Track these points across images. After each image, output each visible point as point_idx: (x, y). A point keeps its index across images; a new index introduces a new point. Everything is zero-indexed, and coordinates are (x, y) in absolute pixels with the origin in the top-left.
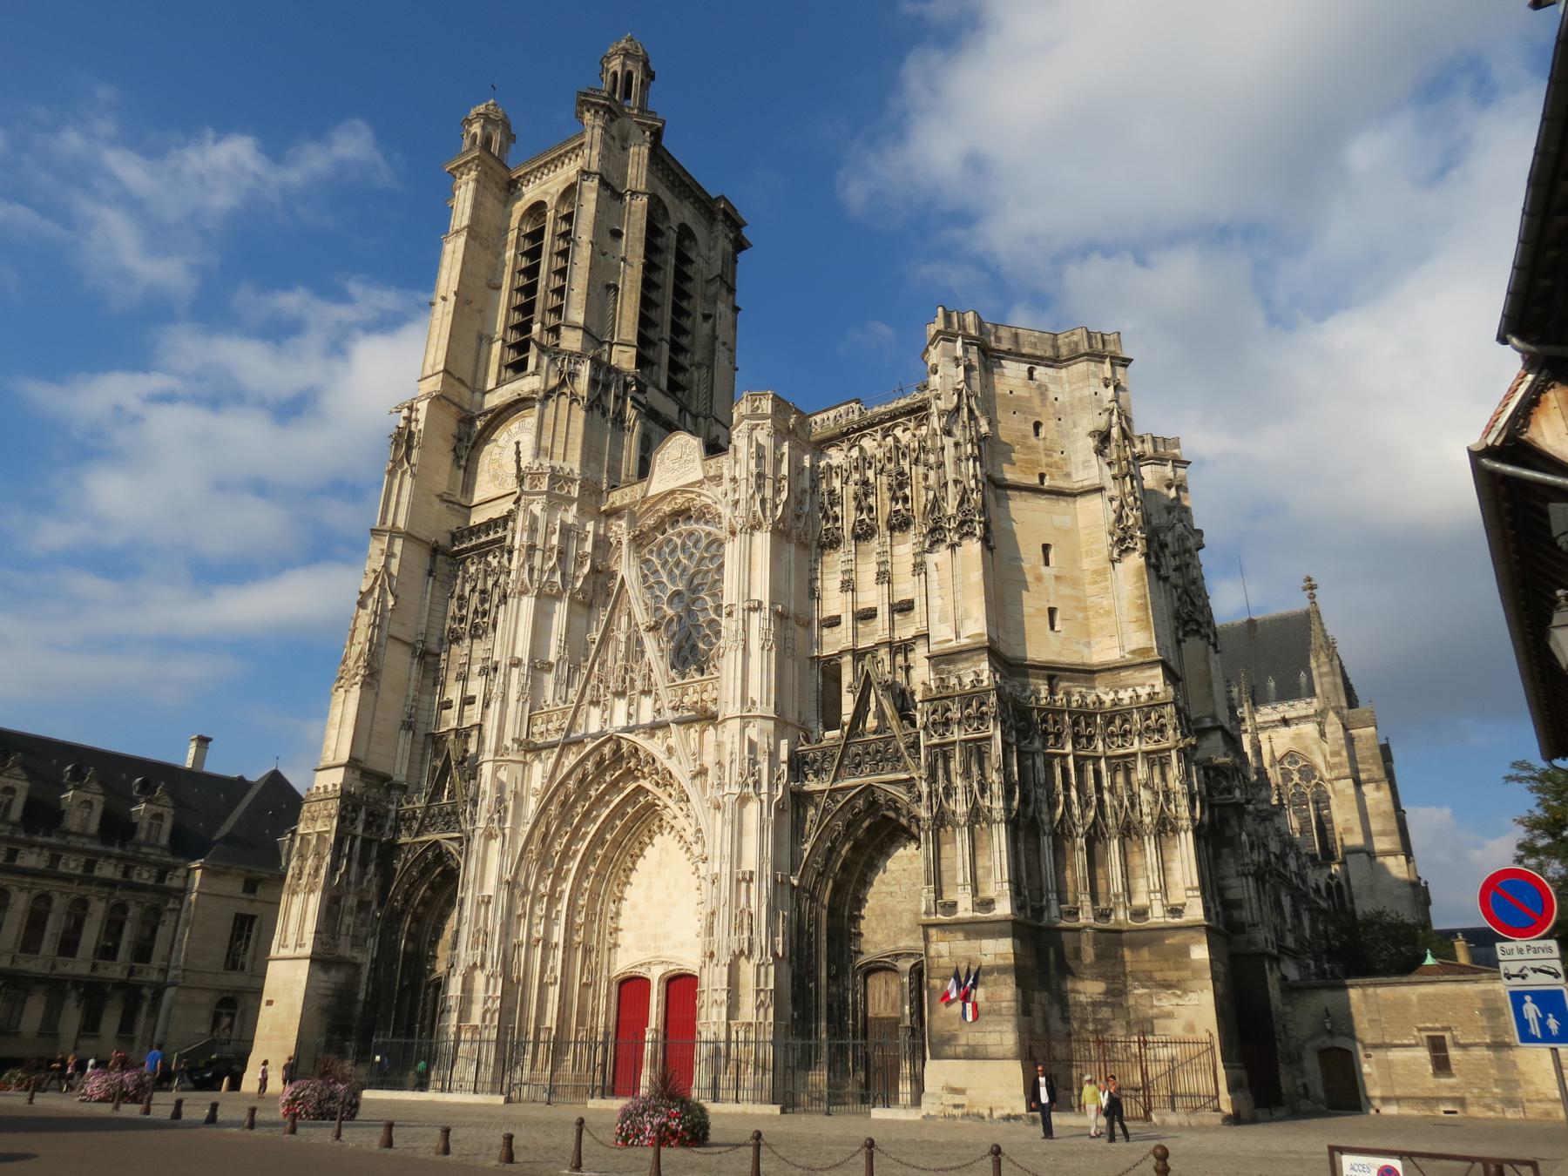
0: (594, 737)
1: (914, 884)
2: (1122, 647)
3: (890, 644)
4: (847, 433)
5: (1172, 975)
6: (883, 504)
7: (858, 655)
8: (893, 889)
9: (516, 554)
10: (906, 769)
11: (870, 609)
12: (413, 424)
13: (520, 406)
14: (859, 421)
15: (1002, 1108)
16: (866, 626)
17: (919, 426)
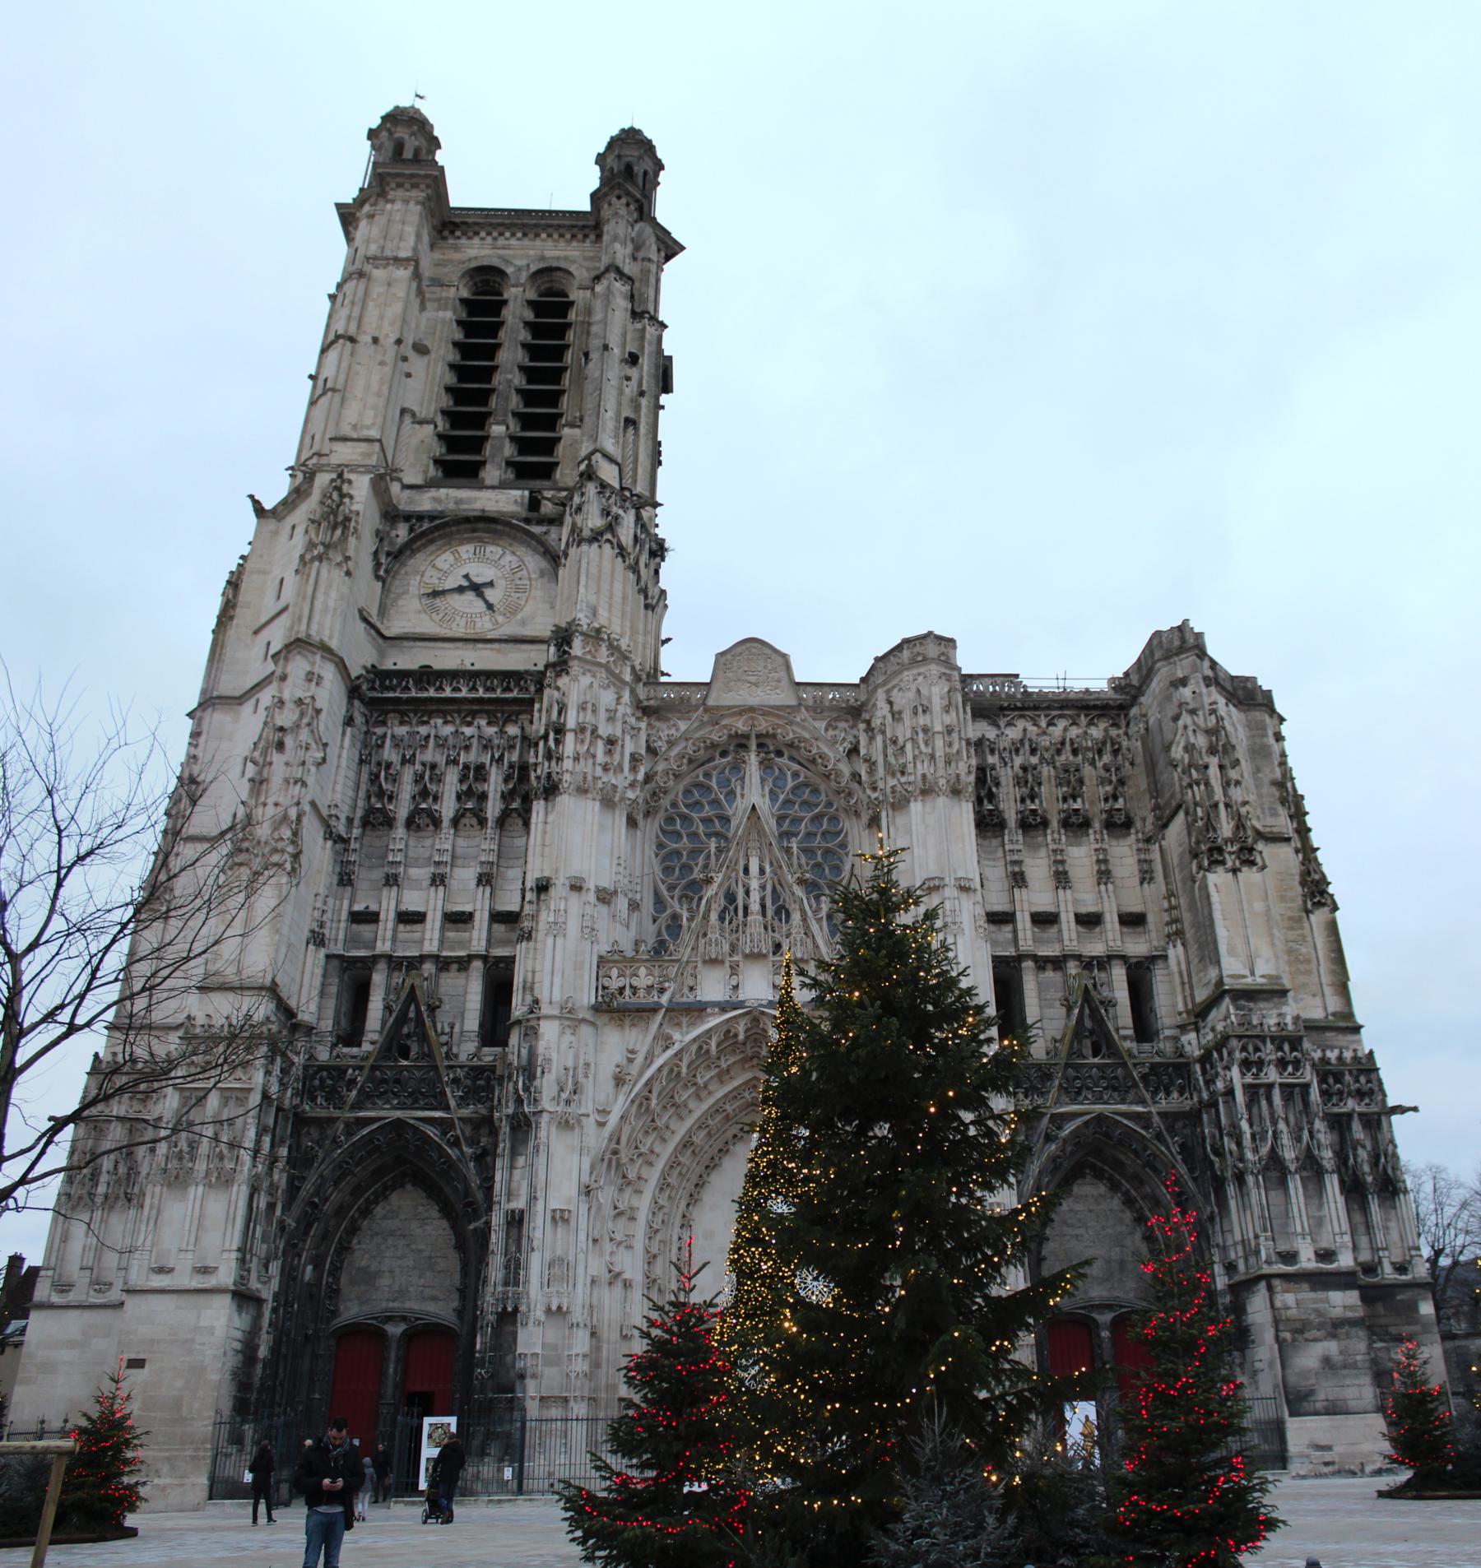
0: (724, 1007)
1: (1104, 1228)
2: (1325, 1008)
3: (1078, 957)
4: (1008, 708)
5: (1406, 1330)
6: (1050, 799)
7: (1042, 963)
8: (1078, 1232)
9: (570, 738)
10: (1143, 1102)
11: (1051, 914)
12: (347, 500)
13: (481, 525)
14: (1023, 702)
15: (1374, 1462)
16: (1043, 931)
17: (1091, 723)
